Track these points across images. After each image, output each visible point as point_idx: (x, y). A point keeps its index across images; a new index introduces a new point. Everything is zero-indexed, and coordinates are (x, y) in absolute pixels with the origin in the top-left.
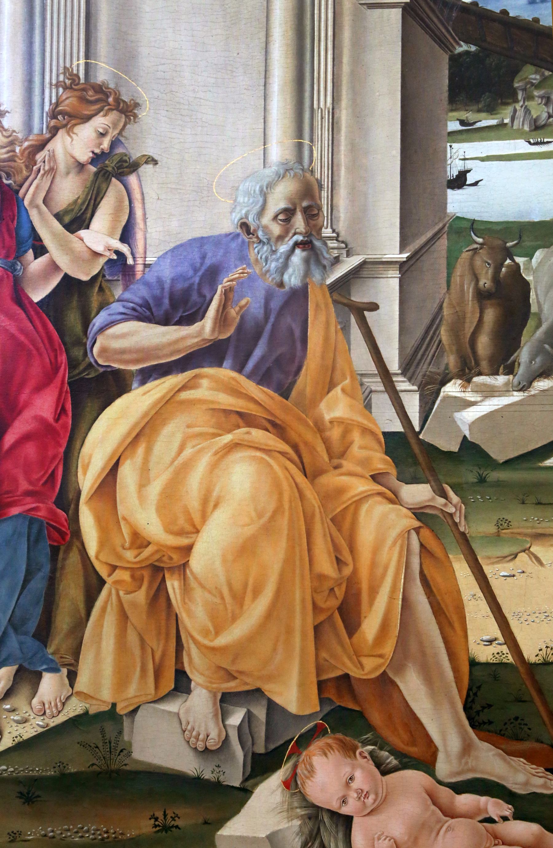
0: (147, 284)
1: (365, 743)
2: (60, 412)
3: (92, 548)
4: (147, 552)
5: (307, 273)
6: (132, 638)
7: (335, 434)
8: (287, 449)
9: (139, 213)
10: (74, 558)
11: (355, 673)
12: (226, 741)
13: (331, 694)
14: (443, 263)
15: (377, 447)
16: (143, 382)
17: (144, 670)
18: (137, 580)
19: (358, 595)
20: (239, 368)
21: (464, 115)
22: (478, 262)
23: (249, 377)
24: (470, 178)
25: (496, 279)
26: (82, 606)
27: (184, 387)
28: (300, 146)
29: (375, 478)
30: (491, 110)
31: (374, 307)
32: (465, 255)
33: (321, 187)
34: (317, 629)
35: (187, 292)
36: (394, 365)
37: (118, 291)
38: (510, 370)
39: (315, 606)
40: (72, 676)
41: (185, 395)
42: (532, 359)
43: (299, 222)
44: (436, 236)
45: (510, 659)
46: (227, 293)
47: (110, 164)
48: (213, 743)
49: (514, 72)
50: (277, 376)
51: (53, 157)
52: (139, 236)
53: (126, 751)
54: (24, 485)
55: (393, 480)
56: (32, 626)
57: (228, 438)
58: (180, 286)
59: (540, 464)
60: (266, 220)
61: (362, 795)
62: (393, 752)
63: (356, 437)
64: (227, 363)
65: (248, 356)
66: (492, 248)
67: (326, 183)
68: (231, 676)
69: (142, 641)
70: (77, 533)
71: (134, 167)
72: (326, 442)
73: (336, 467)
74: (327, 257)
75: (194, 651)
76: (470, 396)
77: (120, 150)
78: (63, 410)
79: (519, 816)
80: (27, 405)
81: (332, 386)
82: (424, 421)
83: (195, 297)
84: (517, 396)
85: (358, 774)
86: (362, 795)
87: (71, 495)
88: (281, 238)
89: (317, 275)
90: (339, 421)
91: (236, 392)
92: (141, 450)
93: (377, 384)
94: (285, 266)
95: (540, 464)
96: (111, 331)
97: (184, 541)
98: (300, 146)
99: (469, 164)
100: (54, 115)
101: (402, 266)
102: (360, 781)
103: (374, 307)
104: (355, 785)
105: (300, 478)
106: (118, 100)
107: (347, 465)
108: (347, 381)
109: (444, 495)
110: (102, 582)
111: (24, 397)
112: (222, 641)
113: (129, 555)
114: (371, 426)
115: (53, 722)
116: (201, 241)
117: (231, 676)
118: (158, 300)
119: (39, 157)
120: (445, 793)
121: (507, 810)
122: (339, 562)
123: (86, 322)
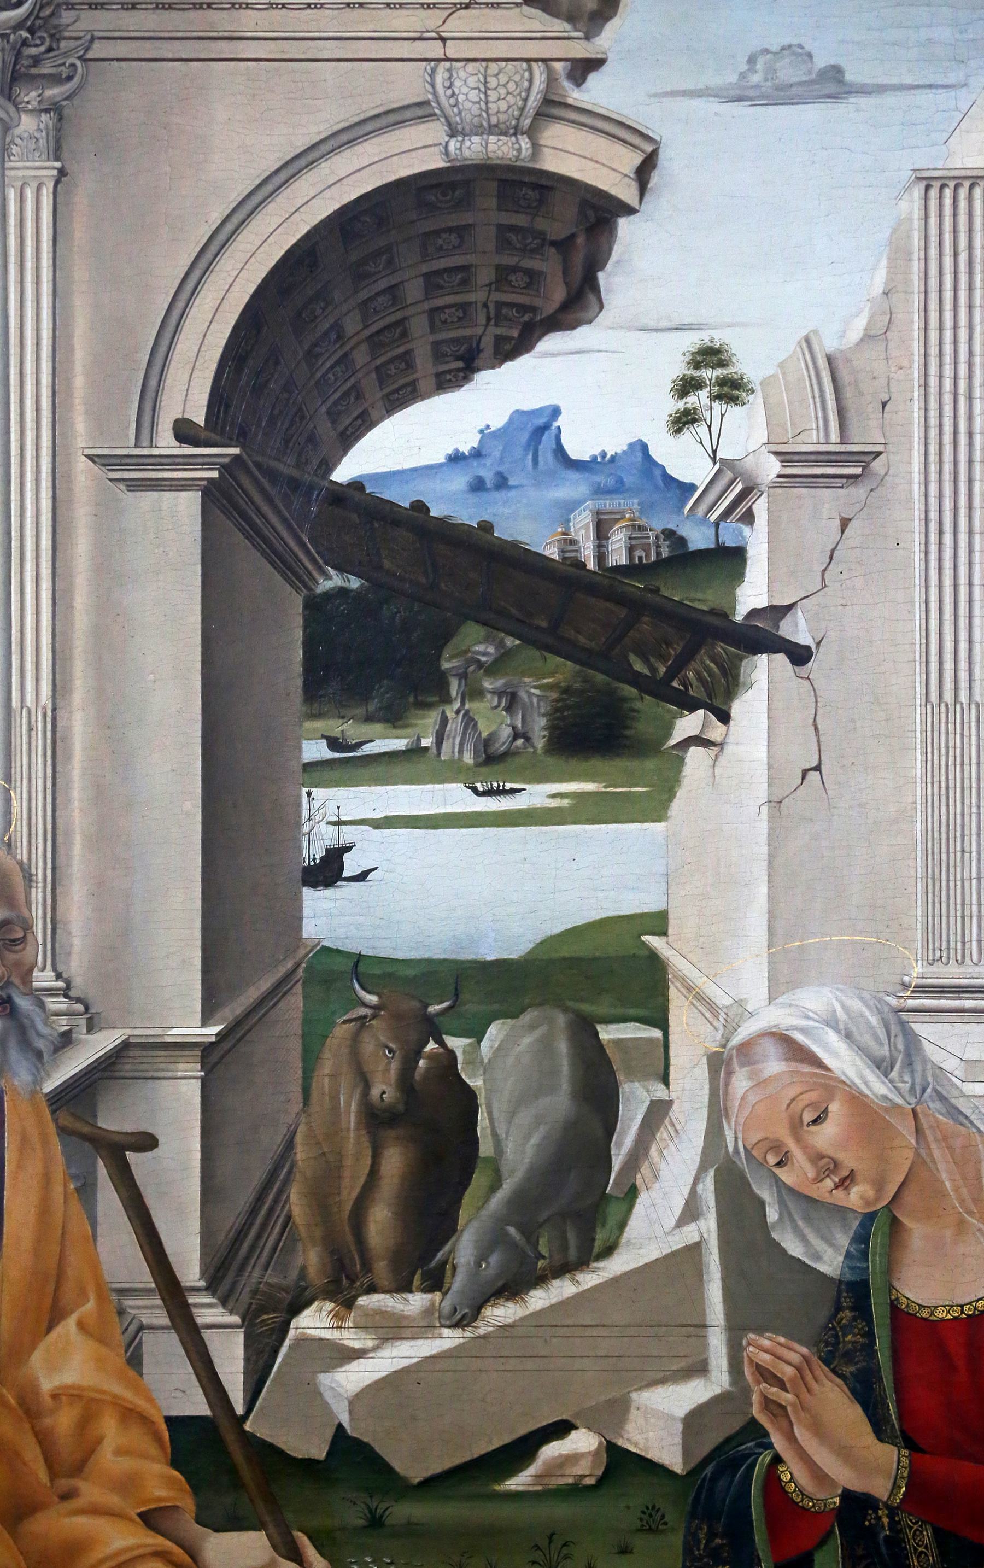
15: (154, 1450)
21: (337, 727)
22: (368, 1046)
24: (351, 865)
25: (406, 1080)
29: (149, 1519)
31: (147, 1142)
32: (341, 1031)
33: (29, 878)
38: (435, 1282)
59: (497, 1488)
66: (398, 1017)
67: (40, 871)
72: (44, 1440)
73: (66, 1496)
76: (351, 1338)
81: (55, 1316)
82: (253, 1392)
84: (450, 1339)
95: (497, 1488)
99: (349, 834)
103: (147, 1142)
107: (90, 1492)
108: (90, 1306)
114: (141, 1403)
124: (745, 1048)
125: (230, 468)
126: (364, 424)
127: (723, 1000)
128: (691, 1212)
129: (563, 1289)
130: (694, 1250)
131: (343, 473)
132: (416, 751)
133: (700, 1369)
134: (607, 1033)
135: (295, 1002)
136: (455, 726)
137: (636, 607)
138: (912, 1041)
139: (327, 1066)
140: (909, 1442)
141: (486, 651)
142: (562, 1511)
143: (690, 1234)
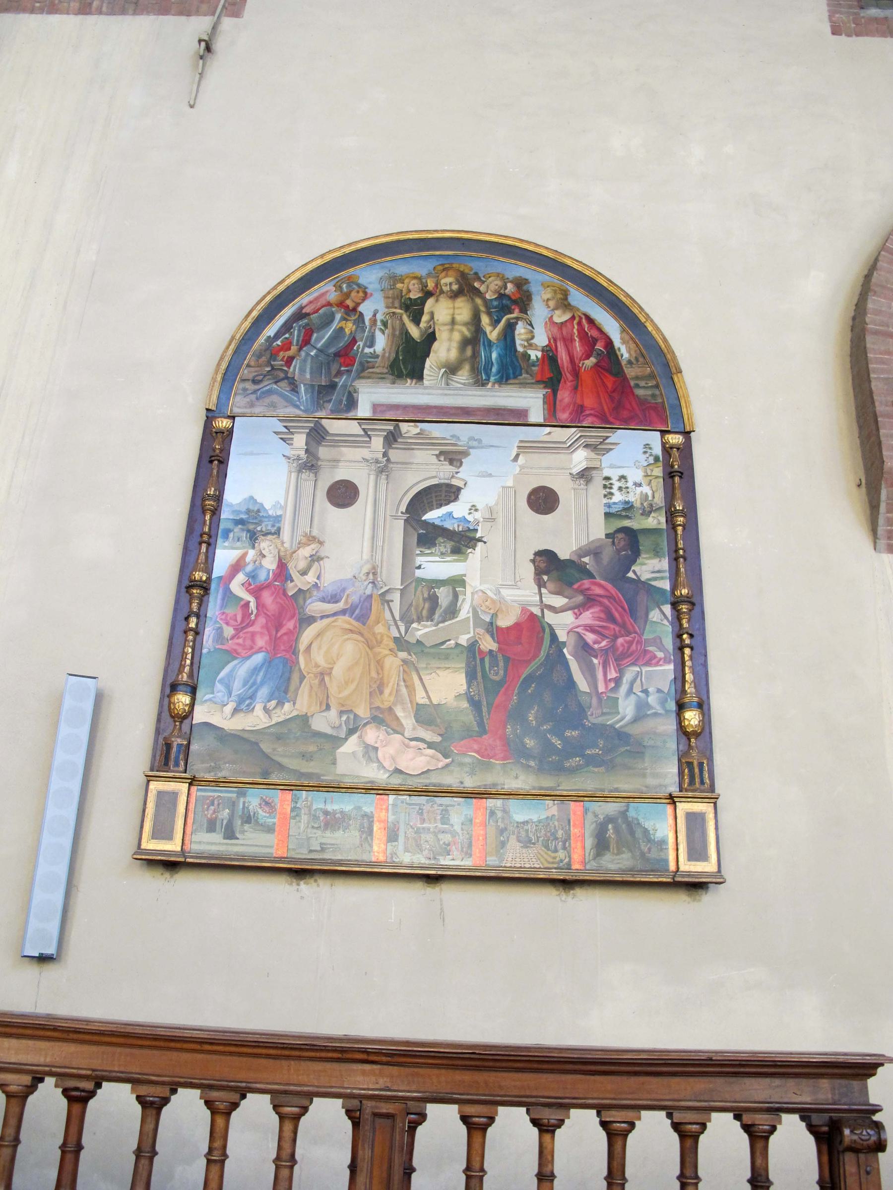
0: (324, 592)
1: (383, 726)
2: (295, 627)
3: (302, 666)
4: (319, 669)
5: (373, 590)
6: (313, 694)
7: (379, 637)
8: (363, 639)
9: (323, 571)
10: (297, 668)
11: (382, 706)
12: (341, 725)
13: (373, 711)
14: (413, 590)
16: (321, 619)
17: (316, 703)
18: (316, 677)
19: (383, 684)
20: (351, 616)
21: (421, 549)
23: (355, 619)
24: (422, 567)
25: (429, 594)
26: (298, 684)
27: (333, 622)
28: (372, 555)
29: (390, 650)
30: (429, 548)
31: (392, 601)
32: (420, 588)
34: (371, 693)
35: (336, 595)
36: (397, 618)
37: (315, 593)
38: (432, 621)
39: (370, 686)
40: (294, 704)
41: (335, 624)
42: (439, 617)
43: (371, 576)
44: (412, 582)
45: (428, 703)
46: (348, 596)
47: (315, 558)
48: (337, 724)
49: (436, 539)
50: (362, 619)
51: (298, 555)
52: (322, 578)
53: (310, 727)
54: (282, 648)
55: (396, 651)
56: (283, 688)
57: (346, 637)
58: (334, 593)
60: (361, 575)
61: (382, 741)
62: (393, 730)
63: (385, 638)
64: (347, 615)
65: (353, 613)
67: (380, 566)
68: (343, 706)
69: (316, 695)
70: (298, 662)
71: (322, 559)
74: (379, 586)
75: (332, 699)
76: (420, 628)
77: (318, 554)
78: (296, 627)
79: (429, 747)
80: (285, 625)
81: (378, 622)
83: (338, 596)
84: (434, 628)
85: (381, 735)
86: (382, 741)
87: (297, 651)
88: (365, 580)
89: (375, 591)
90: (381, 633)
91: (350, 624)
92: (319, 639)
93: (392, 623)
94: (366, 588)
96: (313, 604)
97: (330, 666)
98: (372, 555)
100: (299, 544)
101: (401, 590)
102: (381, 737)
103: (392, 601)
104: (380, 738)
105: (367, 649)
106: (319, 540)
107: (382, 646)
109: (411, 655)
110: (305, 677)
111: (284, 623)
112: (340, 696)
113: (314, 670)
115: (288, 717)
116: (341, 580)
117: (343, 706)
118: (327, 596)
119: (294, 555)
120: (407, 741)
121: (426, 746)
122: (378, 673)
123: (305, 600)
124: (477, 591)
125: (408, 517)
126: (427, 513)
127: (473, 585)
128: (468, 613)
129: (450, 622)
130: (469, 618)
131: (423, 518)
132: (432, 553)
133: (469, 633)
134: (457, 589)
135: (414, 584)
136: (437, 550)
137: (463, 536)
138: (499, 592)
139: (417, 592)
140: (498, 643)
141: (442, 541)
142: (448, 651)
143: (468, 615)
